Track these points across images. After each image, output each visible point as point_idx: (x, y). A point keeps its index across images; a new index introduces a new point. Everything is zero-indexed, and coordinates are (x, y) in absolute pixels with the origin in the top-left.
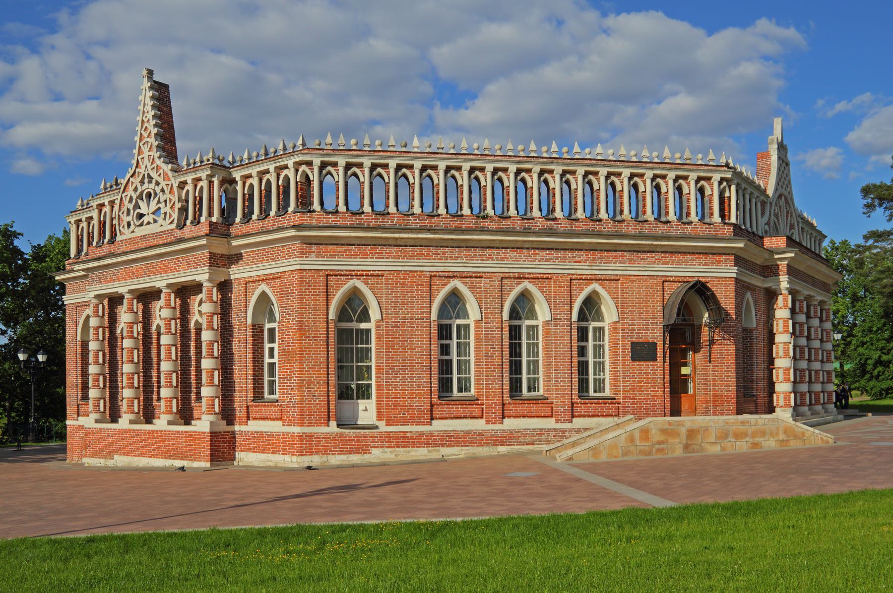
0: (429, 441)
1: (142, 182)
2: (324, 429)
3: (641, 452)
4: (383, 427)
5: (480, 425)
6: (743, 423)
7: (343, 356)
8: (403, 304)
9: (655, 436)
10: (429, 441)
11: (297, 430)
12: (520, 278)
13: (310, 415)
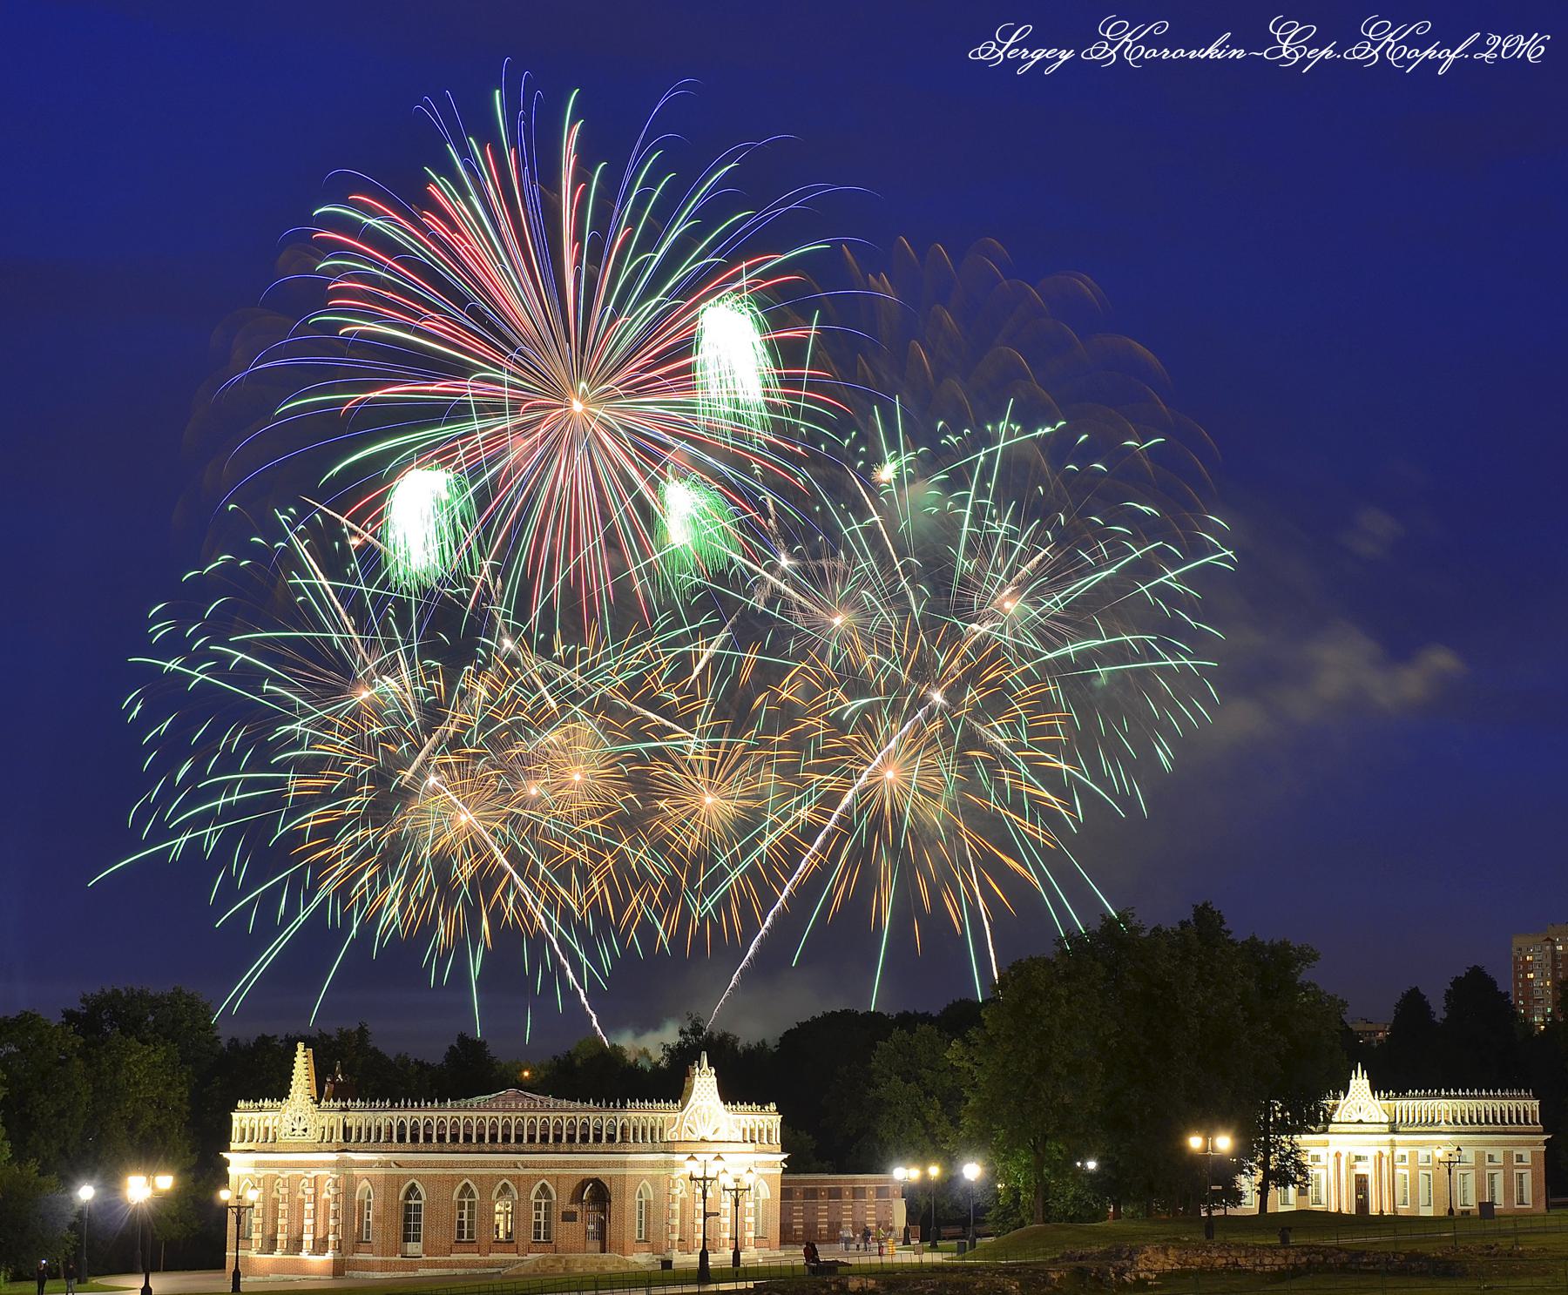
2: (395, 1258)
4: (425, 1257)
5: (476, 1257)
7: (407, 1218)
10: (449, 1265)
11: (380, 1258)
12: (501, 1177)
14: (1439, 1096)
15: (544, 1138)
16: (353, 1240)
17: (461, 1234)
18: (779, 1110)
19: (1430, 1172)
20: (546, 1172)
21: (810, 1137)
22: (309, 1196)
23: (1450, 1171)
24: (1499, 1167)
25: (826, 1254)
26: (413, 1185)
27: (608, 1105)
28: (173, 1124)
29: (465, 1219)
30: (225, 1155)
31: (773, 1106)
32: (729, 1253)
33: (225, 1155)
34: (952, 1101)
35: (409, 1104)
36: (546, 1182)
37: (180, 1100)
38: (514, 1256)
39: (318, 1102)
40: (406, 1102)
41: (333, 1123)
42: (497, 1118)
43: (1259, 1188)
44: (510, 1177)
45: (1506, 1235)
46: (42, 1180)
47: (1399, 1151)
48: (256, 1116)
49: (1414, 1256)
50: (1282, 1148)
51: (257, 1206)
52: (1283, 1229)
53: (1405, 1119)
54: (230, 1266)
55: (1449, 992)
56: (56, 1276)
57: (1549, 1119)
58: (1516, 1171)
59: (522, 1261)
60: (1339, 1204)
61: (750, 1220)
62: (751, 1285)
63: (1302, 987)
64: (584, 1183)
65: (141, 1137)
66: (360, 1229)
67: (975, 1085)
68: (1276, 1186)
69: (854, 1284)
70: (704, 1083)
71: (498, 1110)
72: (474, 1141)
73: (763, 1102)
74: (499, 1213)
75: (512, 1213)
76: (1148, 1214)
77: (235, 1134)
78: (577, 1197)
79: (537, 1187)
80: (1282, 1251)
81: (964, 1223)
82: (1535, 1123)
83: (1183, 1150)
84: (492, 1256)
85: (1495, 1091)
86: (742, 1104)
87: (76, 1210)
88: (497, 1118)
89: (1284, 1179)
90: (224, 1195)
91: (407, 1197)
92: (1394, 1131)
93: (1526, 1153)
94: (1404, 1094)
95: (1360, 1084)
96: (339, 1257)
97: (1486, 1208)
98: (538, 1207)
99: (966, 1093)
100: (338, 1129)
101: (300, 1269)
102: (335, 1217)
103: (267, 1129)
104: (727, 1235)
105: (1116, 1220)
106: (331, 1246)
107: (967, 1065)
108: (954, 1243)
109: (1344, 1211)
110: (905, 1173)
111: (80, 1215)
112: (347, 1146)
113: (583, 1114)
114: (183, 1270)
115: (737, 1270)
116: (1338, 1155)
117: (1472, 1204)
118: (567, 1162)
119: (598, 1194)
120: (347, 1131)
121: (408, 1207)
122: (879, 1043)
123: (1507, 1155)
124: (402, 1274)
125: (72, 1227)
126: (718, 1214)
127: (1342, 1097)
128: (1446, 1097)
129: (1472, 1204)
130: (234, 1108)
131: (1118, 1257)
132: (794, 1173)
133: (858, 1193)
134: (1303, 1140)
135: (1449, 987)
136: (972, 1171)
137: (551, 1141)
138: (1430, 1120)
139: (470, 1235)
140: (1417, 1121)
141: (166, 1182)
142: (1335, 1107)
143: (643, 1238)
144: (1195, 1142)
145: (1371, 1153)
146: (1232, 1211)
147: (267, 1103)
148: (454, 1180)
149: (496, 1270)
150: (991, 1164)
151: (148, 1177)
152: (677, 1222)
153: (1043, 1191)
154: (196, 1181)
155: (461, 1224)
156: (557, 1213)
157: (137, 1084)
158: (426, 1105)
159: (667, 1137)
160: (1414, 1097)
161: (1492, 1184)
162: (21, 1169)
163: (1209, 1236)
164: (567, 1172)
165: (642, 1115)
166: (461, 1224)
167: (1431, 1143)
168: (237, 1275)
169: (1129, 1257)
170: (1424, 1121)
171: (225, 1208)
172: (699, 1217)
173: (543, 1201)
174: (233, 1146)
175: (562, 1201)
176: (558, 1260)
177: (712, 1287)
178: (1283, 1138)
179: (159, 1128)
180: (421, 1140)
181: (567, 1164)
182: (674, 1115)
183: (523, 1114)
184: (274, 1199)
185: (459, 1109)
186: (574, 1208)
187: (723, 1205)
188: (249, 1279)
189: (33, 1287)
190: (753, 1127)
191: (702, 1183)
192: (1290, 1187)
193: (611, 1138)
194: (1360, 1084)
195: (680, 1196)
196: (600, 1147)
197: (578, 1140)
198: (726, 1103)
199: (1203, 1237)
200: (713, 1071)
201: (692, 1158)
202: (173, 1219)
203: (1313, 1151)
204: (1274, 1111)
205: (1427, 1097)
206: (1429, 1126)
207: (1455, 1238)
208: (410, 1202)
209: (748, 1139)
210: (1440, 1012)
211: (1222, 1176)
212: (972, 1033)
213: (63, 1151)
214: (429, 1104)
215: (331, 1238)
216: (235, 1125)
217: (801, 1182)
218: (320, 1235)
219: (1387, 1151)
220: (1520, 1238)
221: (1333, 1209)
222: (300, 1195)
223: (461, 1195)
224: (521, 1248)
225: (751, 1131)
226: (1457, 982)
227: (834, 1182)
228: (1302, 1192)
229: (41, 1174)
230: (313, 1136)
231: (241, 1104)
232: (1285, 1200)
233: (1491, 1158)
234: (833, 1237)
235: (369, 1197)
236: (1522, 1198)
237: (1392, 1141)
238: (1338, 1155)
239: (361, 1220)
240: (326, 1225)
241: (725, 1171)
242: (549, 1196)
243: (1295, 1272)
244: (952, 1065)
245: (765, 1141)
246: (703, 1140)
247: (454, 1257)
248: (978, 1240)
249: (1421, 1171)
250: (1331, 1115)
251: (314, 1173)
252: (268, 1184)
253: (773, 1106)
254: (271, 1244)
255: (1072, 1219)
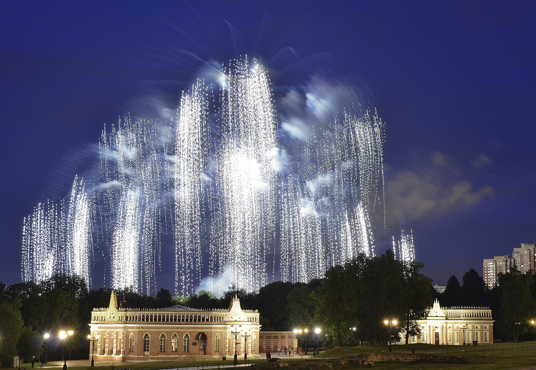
4: (150, 356)
5: (166, 356)
7: (145, 344)
10: (158, 358)
11: (136, 356)
12: (174, 332)
14: (461, 309)
15: (187, 320)
16: (128, 351)
17: (161, 349)
18: (259, 312)
19: (458, 332)
20: (187, 330)
21: (268, 320)
22: (115, 337)
23: (464, 331)
24: (479, 330)
25: (273, 356)
26: (147, 335)
27: (206, 310)
28: (73, 315)
29: (163, 344)
30: (89, 325)
31: (257, 311)
32: (243, 355)
33: (89, 325)
34: (312, 309)
35: (146, 309)
36: (187, 333)
37: (76, 308)
38: (178, 356)
39: (118, 309)
40: (145, 309)
41: (122, 315)
42: (173, 314)
43: (405, 336)
44: (176, 332)
45: (480, 351)
46: (33, 332)
47: (448, 325)
48: (99, 312)
49: (452, 357)
50: (413, 324)
51: (99, 340)
52: (413, 349)
53: (450, 316)
54: (91, 359)
55: (464, 277)
56: (37, 361)
57: (494, 316)
58: (484, 331)
59: (180, 357)
60: (430, 341)
61: (250, 345)
62: (250, 365)
63: (419, 275)
64: (199, 334)
65: (64, 319)
66: (131, 347)
67: (319, 305)
68: (411, 336)
69: (281, 365)
70: (236, 304)
71: (173, 311)
72: (166, 321)
73: (254, 309)
74: (173, 343)
75: (177, 343)
76: (372, 344)
77: (93, 318)
78: (197, 338)
79: (185, 335)
80: (413, 356)
81: (315, 346)
82: (490, 317)
83: (383, 324)
84: (171, 356)
85: (478, 307)
86: (247, 310)
87: (44, 341)
88: (173, 314)
89: (413, 333)
90: (89, 337)
91: (145, 338)
92: (447, 319)
93: (487, 326)
94: (450, 308)
95: (436, 305)
96: (124, 356)
97: (475, 343)
98: (185, 341)
99: (316, 307)
100: (124, 317)
101: (112, 359)
102: (123, 344)
103: (102, 317)
104: (243, 350)
105: (362, 346)
106: (121, 353)
107: (316, 298)
108: (312, 353)
109: (432, 343)
110: (297, 331)
111: (45, 342)
112: (127, 322)
113: (199, 313)
114: (76, 360)
115: (246, 361)
116: (430, 326)
117: (471, 341)
118: (194, 327)
119: (203, 337)
120: (127, 317)
121: (145, 341)
122: (290, 291)
123: (482, 327)
124: (143, 361)
125: (42, 346)
126: (240, 343)
127: (431, 308)
128: (463, 309)
129: (471, 341)
130: (92, 310)
131: (362, 357)
132: (263, 331)
133: (283, 337)
134: (419, 322)
135: (464, 275)
136: (318, 331)
137: (189, 321)
138: (458, 316)
139: (164, 349)
140: (454, 316)
141: (71, 333)
142: (429, 312)
144: (386, 322)
145: (440, 326)
146: (397, 343)
147: (102, 309)
148: (159, 333)
149: (172, 360)
150: (323, 328)
151: (66, 331)
152: (227, 346)
153: (339, 337)
154: (80, 332)
155: (161, 346)
157: (62, 303)
158: (151, 310)
159: (225, 320)
160: (453, 309)
161: (477, 335)
162: (27, 329)
163: (390, 351)
164: (194, 330)
165: (217, 313)
166: (161, 346)
167: (459, 323)
168: (93, 361)
169: (366, 357)
170: (456, 316)
171: (89, 341)
172: (234, 344)
173: (187, 339)
174: (92, 322)
175: (192, 339)
176: (191, 357)
177: (238, 366)
178: (413, 321)
179: (69, 316)
180: (149, 320)
181: (194, 328)
182: (226, 313)
183: (180, 313)
184: (104, 338)
185: (161, 311)
186: (196, 341)
187: (242, 341)
188: (97, 362)
189: (30, 365)
190: (251, 317)
191: (235, 334)
192: (415, 336)
193: (207, 320)
194: (436, 305)
195: (228, 338)
196: (204, 323)
197: (197, 321)
198: (242, 310)
199: (388, 351)
200: (239, 300)
201: (232, 326)
202: (73, 344)
203: (422, 325)
204: (410, 313)
205: (457, 309)
206: (458, 317)
207: (465, 352)
208: (146, 339)
209: (249, 320)
210: (461, 284)
211: (394, 333)
212: (318, 289)
213: (40, 323)
214: (152, 309)
215: (122, 350)
216: (93, 315)
217: (265, 334)
218: (118, 349)
219: (445, 325)
220: (485, 352)
221: (428, 343)
222: (112, 337)
223: (162, 337)
224: (180, 354)
225: (250, 318)
226: (467, 274)
227: (275, 334)
228: (419, 338)
229: (33, 330)
230: (116, 319)
231: (94, 309)
232: (414, 340)
233: (477, 327)
234: (275, 351)
235: (133, 338)
236: (486, 340)
237: (446, 322)
238: (430, 326)
239: (131, 345)
240: (120, 346)
241: (242, 330)
242: (188, 338)
243: (416, 362)
244: (312, 298)
245: (255, 321)
246: (236, 321)
247: (159, 356)
248: (320, 352)
249: (455, 331)
250: (428, 314)
251: (117, 330)
252: (102, 334)
253: (257, 311)
254: (103, 352)
255: (348, 345)
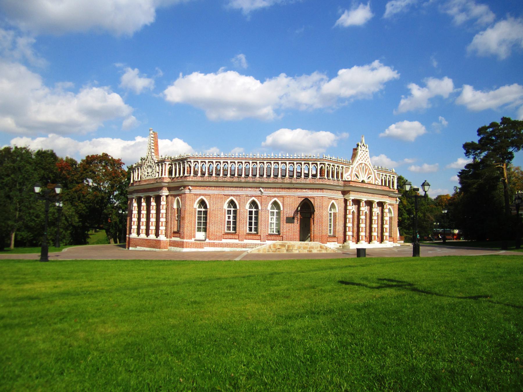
0: (222, 245)
1: (148, 162)
3: (273, 251)
5: (236, 241)
6: (306, 244)
8: (215, 204)
9: (278, 247)
13: (187, 236)
59: (263, 244)
84: (246, 241)
143: (332, 234)
156: (283, 217)
224: (262, 237)
242: (278, 207)
